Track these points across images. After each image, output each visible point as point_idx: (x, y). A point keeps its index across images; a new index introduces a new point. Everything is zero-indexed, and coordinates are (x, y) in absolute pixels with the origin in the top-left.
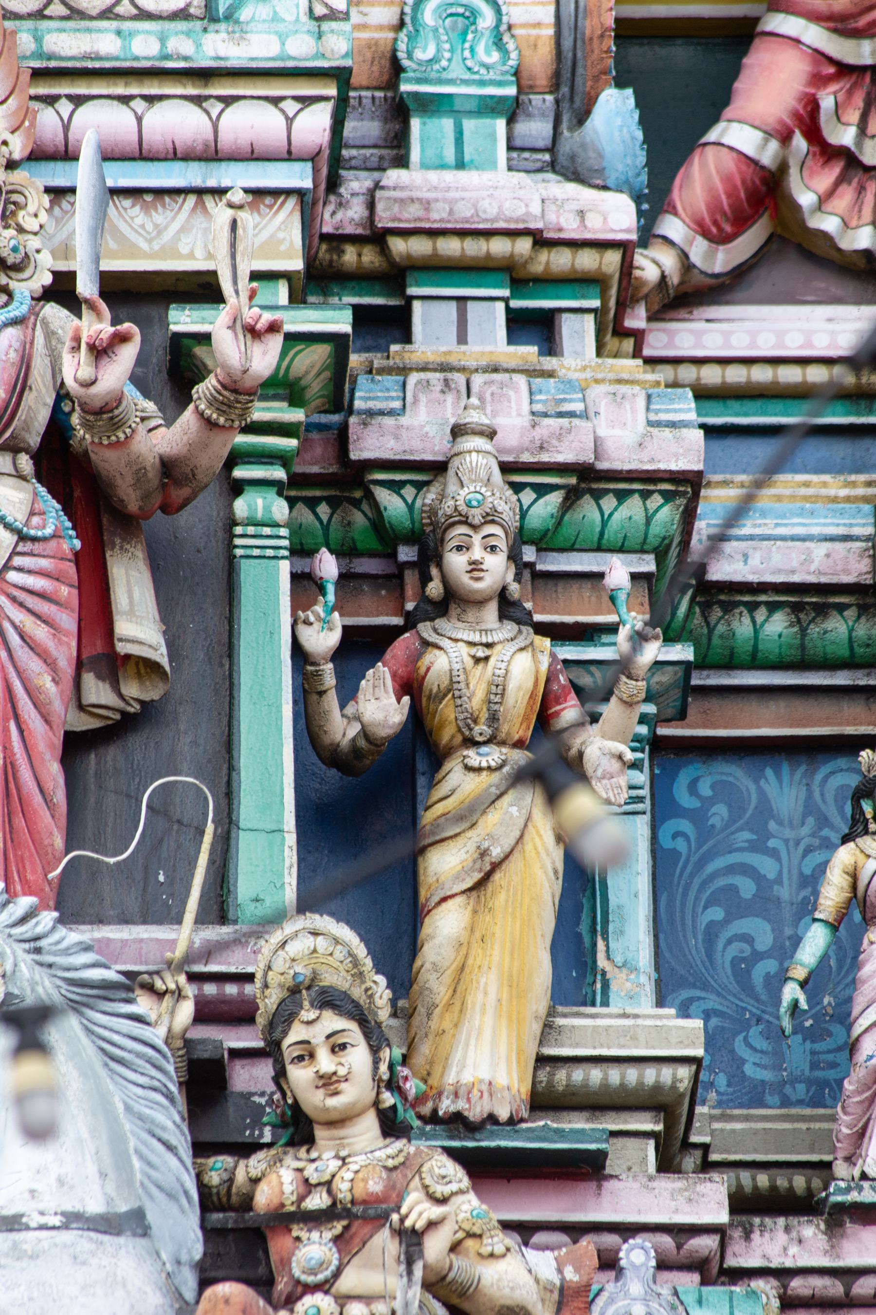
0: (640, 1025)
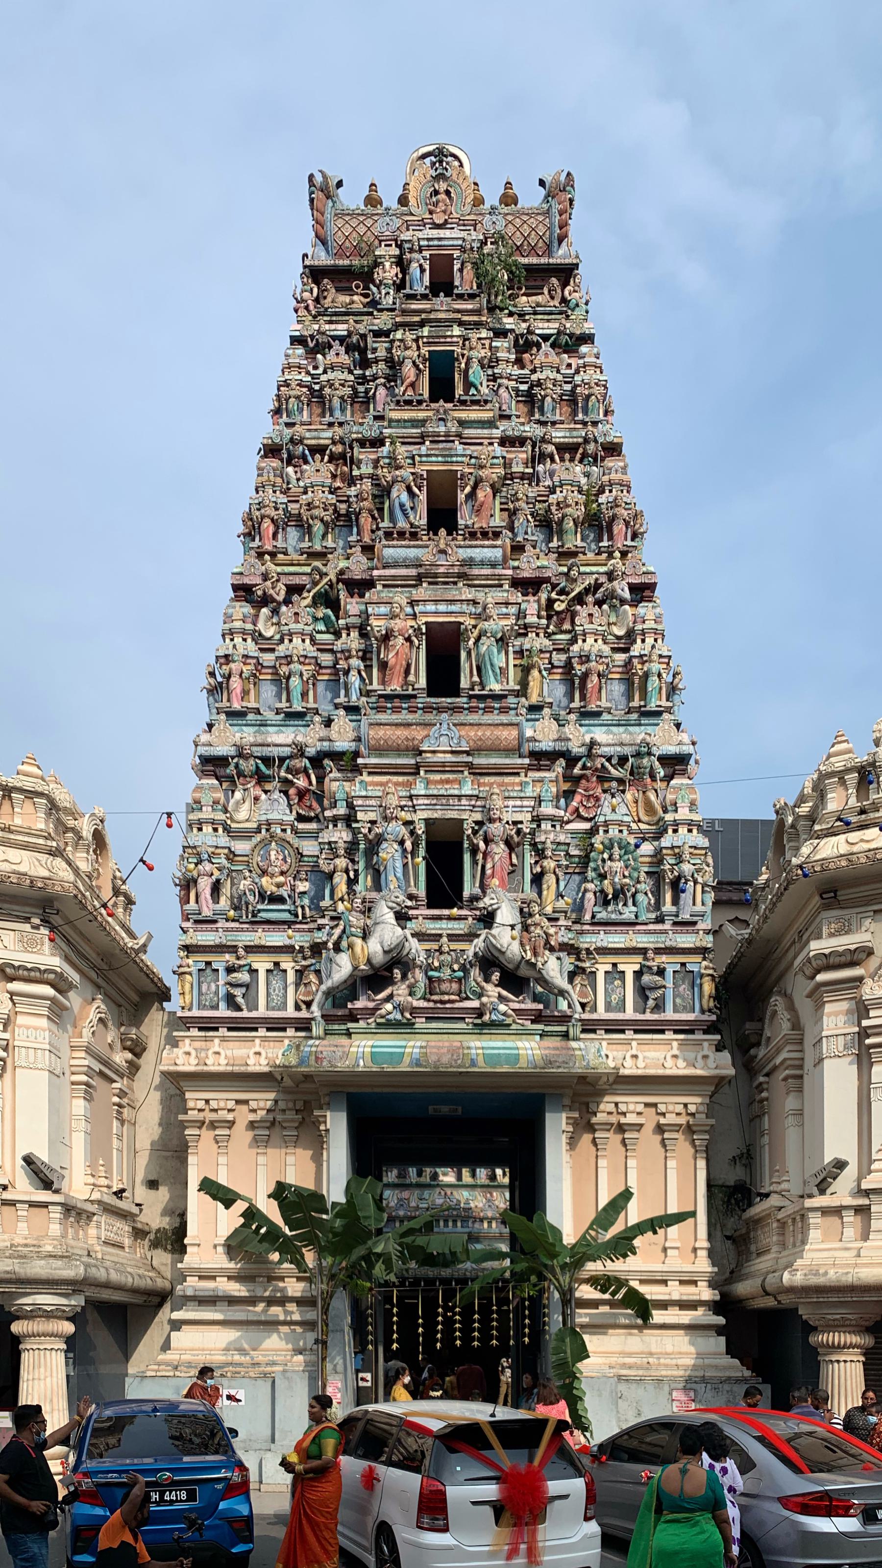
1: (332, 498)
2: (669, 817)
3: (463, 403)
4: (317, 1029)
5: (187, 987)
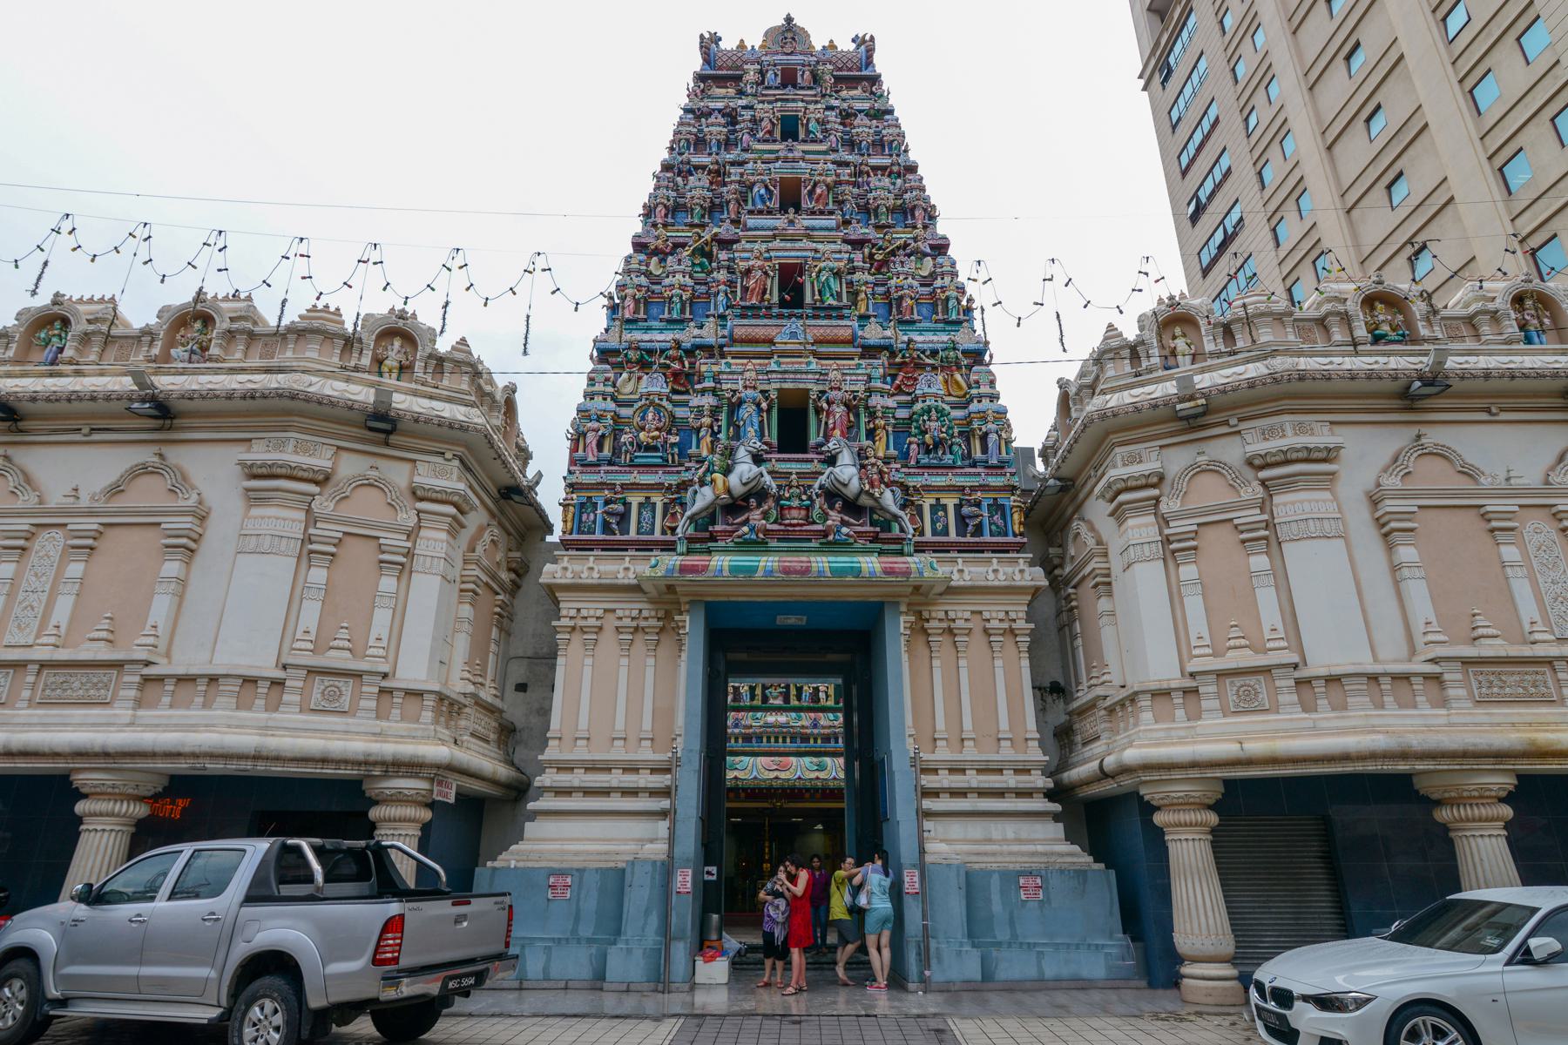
0: (892, 452)
1: (710, 194)
2: (974, 391)
3: (804, 141)
4: (681, 548)
5: (570, 516)
